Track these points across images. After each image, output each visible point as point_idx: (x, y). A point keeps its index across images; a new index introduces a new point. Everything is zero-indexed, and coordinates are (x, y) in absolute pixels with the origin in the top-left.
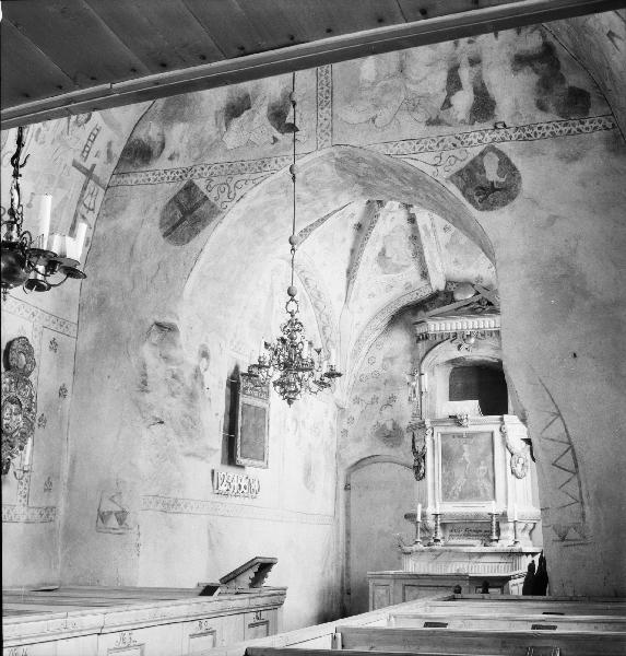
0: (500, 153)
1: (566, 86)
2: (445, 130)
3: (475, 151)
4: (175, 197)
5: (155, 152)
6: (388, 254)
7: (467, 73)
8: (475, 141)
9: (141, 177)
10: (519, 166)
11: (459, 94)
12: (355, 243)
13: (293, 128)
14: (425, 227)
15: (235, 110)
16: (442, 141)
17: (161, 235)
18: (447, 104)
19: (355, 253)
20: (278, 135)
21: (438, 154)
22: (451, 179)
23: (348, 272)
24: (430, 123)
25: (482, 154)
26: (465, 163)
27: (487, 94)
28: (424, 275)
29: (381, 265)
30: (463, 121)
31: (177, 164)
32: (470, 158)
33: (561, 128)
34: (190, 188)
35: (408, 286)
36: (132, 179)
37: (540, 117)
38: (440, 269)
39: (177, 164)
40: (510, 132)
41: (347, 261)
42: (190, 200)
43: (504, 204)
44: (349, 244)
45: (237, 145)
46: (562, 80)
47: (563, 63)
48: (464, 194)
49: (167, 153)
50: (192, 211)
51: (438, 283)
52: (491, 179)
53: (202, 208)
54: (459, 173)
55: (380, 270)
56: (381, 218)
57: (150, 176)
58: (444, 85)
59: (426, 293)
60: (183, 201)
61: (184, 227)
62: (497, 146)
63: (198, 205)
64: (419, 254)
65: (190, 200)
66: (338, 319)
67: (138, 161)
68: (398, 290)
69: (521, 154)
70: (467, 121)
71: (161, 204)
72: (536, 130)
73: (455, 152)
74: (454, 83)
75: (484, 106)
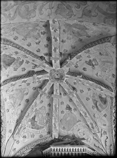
6: (36, 120)
12: (24, 109)
14: (56, 105)
19: (23, 113)
23: (17, 121)
28: (50, 132)
29: (31, 123)
35: (41, 136)
38: (57, 128)
41: (18, 116)
44: (22, 107)
51: (55, 135)
55: (31, 126)
56: (39, 95)
59: (50, 139)
64: (49, 121)
66: (6, 141)
68: (37, 137)
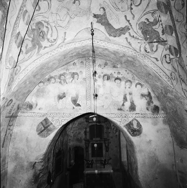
0: (137, 121)
1: (154, 104)
2: (123, 112)
3: (130, 119)
4: (41, 122)
5: (34, 107)
7: (129, 97)
8: (131, 116)
9: (29, 114)
10: (142, 125)
11: (126, 102)
13: (79, 105)
15: (61, 97)
16: (122, 115)
17: (37, 134)
18: (123, 105)
20: (74, 106)
21: (121, 118)
22: (124, 126)
24: (118, 109)
25: (133, 120)
26: (128, 122)
27: (133, 104)
30: (127, 110)
31: (41, 111)
32: (130, 121)
33: (152, 116)
34: (46, 120)
36: (26, 114)
37: (147, 112)
39: (41, 111)
40: (140, 115)
42: (46, 123)
43: (139, 135)
45: (61, 108)
46: (152, 103)
47: (153, 98)
48: (128, 131)
49: (38, 107)
50: (47, 127)
52: (135, 128)
53: (51, 126)
54: (127, 125)
57: (33, 114)
58: (122, 99)
60: (44, 123)
61: (45, 132)
62: (136, 119)
63: (49, 126)
65: (46, 123)
67: (28, 109)
69: (142, 121)
70: (129, 110)
71: (37, 124)
72: (146, 115)
73: (126, 119)
74: (125, 99)
75: (133, 108)
